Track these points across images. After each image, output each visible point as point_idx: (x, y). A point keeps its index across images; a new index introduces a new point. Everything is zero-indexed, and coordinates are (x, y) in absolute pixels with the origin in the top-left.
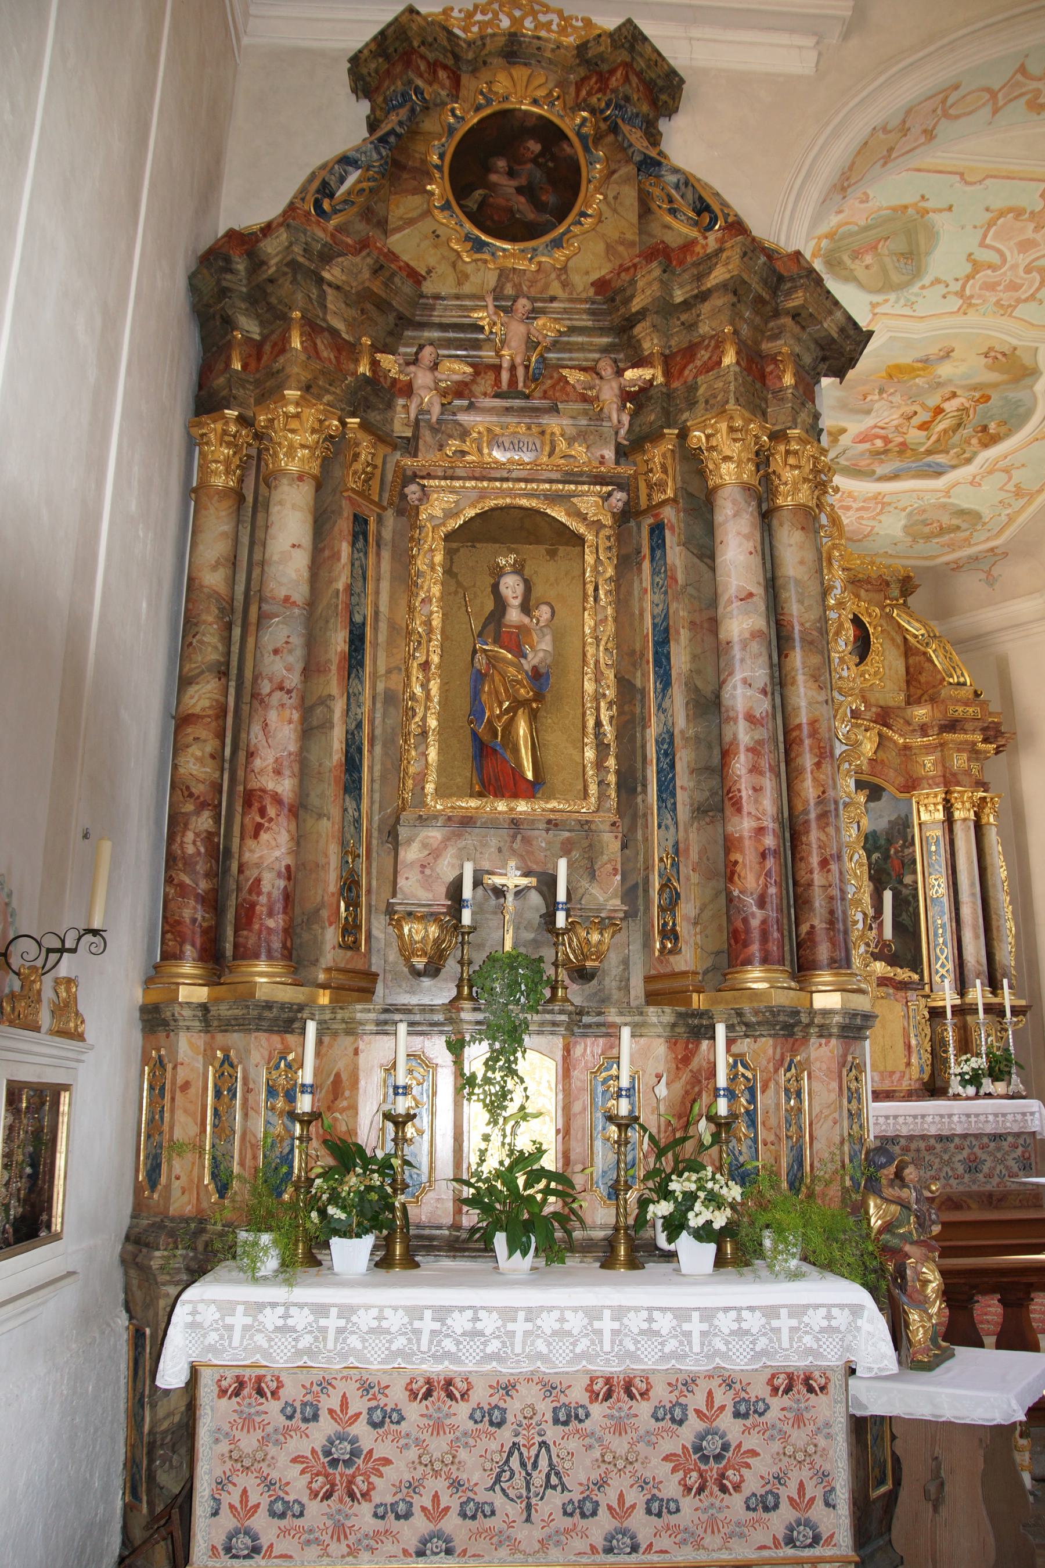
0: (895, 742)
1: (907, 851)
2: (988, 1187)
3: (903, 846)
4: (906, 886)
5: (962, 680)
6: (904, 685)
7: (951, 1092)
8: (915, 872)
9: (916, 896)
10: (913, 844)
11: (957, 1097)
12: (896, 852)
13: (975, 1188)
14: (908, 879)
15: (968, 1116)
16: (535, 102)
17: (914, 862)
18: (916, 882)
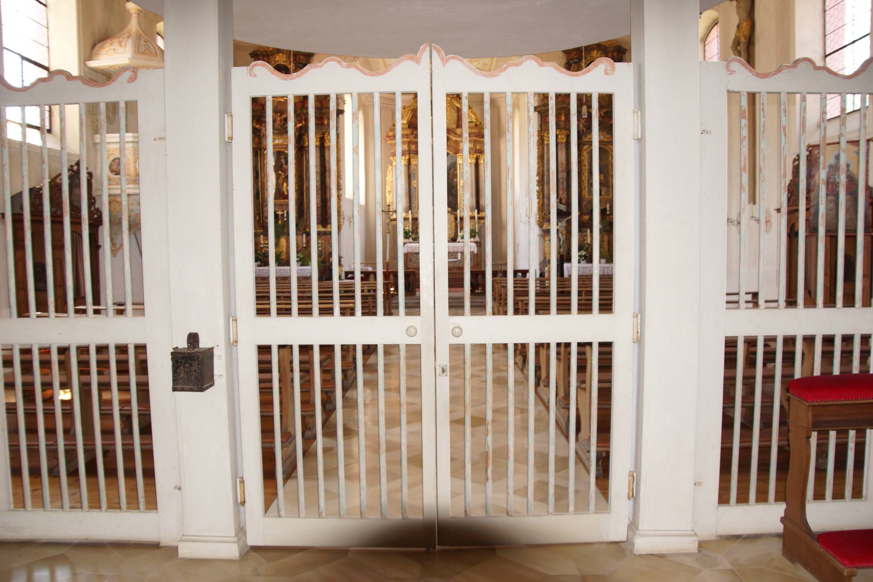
0: (453, 139)
1: (455, 172)
2: (459, 265)
3: (454, 171)
4: (454, 182)
5: (472, 120)
6: (456, 122)
7: (458, 241)
8: (457, 178)
9: (457, 185)
10: (457, 169)
11: (459, 242)
12: (452, 172)
13: (456, 265)
14: (455, 180)
15: (454, 247)
16: (284, 62)
17: (457, 175)
18: (457, 181)
